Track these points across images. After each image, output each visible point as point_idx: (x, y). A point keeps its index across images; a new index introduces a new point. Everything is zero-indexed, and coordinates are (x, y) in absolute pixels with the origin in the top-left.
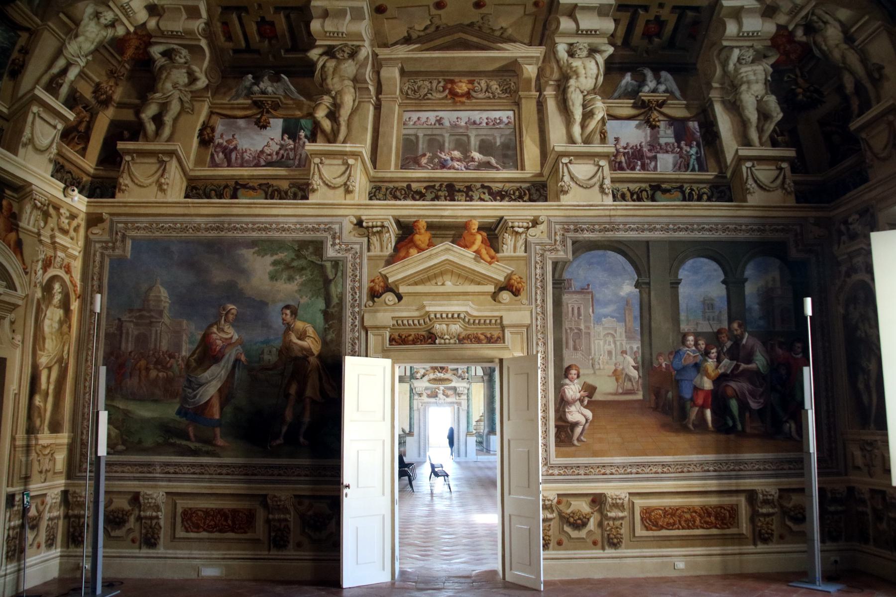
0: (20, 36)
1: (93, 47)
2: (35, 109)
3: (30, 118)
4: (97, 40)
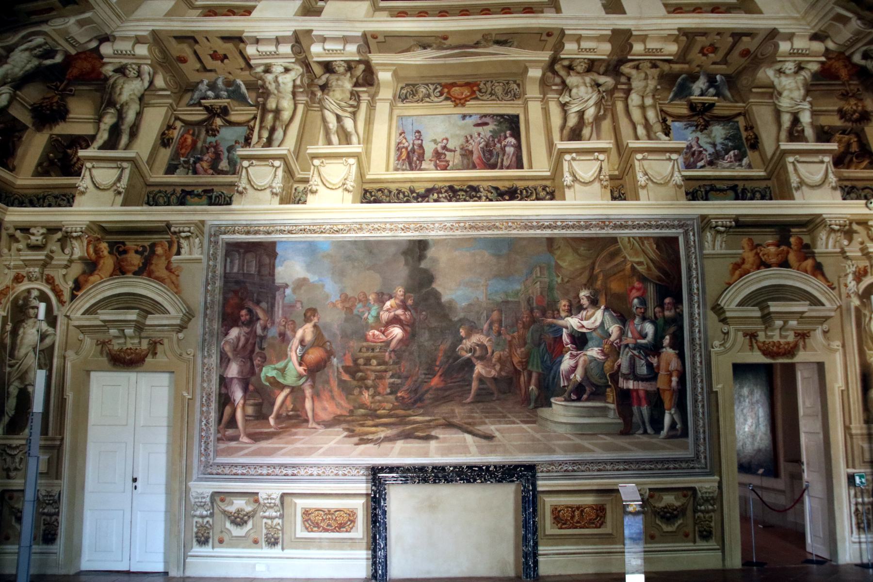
0: (737, 122)
1: (802, 92)
2: (791, 159)
3: (790, 168)
4: (800, 85)
